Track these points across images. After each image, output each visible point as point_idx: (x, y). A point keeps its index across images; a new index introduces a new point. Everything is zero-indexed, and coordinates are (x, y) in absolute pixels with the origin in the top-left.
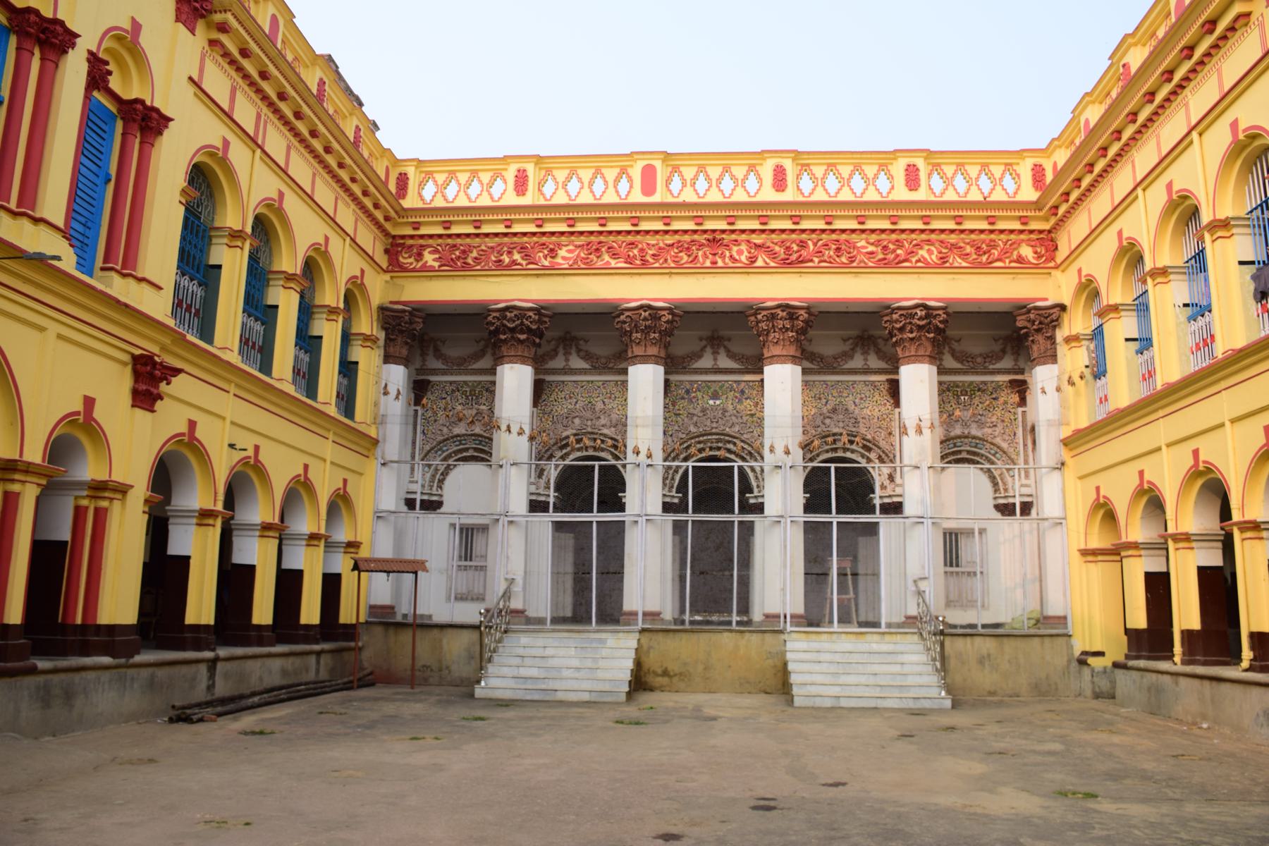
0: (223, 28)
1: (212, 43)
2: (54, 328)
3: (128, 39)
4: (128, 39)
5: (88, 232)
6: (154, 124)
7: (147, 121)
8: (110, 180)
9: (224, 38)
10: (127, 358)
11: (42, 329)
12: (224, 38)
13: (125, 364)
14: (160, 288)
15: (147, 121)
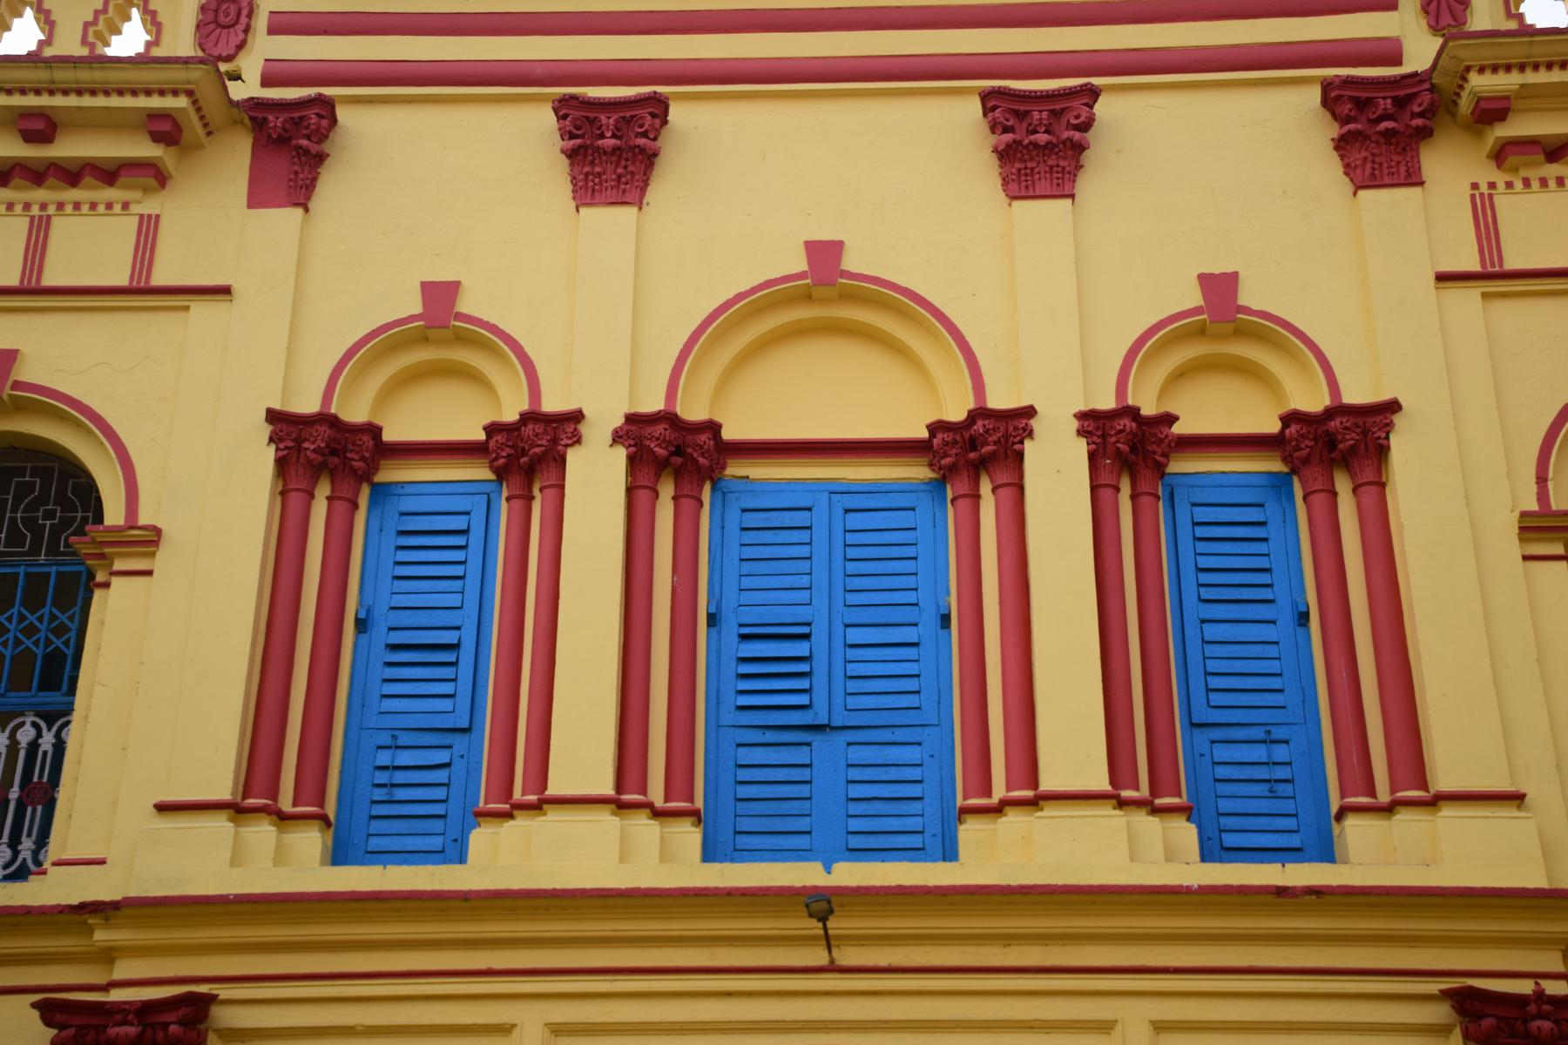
0: (1492, 111)
1: (1501, 154)
2: (1134, 1017)
3: (1220, 316)
4: (1220, 316)
5: (1280, 753)
6: (1350, 439)
7: (1342, 444)
8: (1303, 618)
9: (1518, 127)
10: (1441, 1013)
11: (1106, 1027)
12: (1518, 127)
13: (1442, 1030)
14: (1516, 798)
15: (1342, 444)
